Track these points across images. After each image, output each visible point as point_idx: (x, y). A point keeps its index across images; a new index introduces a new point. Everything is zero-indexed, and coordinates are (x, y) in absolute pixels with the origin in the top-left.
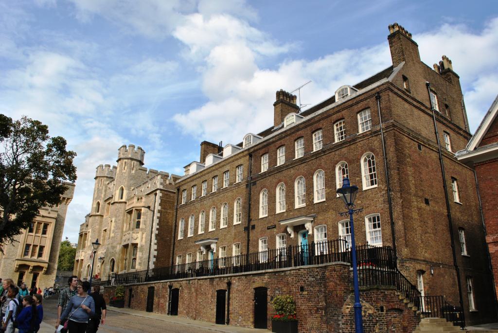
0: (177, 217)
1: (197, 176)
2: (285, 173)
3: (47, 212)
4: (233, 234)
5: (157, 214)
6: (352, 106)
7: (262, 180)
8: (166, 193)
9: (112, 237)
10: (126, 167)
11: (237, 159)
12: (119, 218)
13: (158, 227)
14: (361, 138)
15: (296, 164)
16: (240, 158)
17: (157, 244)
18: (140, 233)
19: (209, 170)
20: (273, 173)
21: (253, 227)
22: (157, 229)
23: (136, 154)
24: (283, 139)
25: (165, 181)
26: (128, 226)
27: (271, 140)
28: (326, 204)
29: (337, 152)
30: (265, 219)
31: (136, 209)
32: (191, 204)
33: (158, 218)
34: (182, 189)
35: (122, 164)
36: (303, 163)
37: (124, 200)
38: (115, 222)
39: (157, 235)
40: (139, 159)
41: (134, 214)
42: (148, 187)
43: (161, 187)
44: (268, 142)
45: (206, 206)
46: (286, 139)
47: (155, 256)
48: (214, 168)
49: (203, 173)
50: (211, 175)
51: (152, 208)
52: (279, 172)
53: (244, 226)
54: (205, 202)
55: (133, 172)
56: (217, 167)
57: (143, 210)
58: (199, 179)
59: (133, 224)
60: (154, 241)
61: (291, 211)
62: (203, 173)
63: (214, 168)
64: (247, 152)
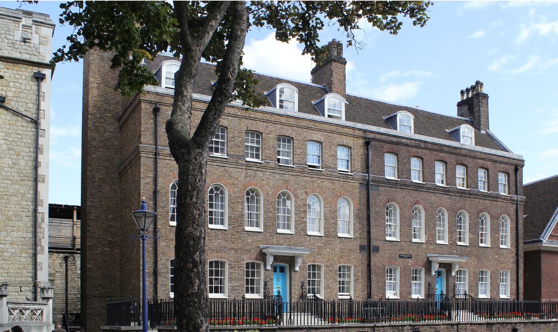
6: (496, 162)
7: (389, 189)
14: (502, 199)
20: (409, 188)
24: (420, 150)
27: (404, 141)
28: (469, 249)
29: (481, 201)
30: (395, 243)
44: (400, 140)
48: (283, 120)
52: (417, 190)
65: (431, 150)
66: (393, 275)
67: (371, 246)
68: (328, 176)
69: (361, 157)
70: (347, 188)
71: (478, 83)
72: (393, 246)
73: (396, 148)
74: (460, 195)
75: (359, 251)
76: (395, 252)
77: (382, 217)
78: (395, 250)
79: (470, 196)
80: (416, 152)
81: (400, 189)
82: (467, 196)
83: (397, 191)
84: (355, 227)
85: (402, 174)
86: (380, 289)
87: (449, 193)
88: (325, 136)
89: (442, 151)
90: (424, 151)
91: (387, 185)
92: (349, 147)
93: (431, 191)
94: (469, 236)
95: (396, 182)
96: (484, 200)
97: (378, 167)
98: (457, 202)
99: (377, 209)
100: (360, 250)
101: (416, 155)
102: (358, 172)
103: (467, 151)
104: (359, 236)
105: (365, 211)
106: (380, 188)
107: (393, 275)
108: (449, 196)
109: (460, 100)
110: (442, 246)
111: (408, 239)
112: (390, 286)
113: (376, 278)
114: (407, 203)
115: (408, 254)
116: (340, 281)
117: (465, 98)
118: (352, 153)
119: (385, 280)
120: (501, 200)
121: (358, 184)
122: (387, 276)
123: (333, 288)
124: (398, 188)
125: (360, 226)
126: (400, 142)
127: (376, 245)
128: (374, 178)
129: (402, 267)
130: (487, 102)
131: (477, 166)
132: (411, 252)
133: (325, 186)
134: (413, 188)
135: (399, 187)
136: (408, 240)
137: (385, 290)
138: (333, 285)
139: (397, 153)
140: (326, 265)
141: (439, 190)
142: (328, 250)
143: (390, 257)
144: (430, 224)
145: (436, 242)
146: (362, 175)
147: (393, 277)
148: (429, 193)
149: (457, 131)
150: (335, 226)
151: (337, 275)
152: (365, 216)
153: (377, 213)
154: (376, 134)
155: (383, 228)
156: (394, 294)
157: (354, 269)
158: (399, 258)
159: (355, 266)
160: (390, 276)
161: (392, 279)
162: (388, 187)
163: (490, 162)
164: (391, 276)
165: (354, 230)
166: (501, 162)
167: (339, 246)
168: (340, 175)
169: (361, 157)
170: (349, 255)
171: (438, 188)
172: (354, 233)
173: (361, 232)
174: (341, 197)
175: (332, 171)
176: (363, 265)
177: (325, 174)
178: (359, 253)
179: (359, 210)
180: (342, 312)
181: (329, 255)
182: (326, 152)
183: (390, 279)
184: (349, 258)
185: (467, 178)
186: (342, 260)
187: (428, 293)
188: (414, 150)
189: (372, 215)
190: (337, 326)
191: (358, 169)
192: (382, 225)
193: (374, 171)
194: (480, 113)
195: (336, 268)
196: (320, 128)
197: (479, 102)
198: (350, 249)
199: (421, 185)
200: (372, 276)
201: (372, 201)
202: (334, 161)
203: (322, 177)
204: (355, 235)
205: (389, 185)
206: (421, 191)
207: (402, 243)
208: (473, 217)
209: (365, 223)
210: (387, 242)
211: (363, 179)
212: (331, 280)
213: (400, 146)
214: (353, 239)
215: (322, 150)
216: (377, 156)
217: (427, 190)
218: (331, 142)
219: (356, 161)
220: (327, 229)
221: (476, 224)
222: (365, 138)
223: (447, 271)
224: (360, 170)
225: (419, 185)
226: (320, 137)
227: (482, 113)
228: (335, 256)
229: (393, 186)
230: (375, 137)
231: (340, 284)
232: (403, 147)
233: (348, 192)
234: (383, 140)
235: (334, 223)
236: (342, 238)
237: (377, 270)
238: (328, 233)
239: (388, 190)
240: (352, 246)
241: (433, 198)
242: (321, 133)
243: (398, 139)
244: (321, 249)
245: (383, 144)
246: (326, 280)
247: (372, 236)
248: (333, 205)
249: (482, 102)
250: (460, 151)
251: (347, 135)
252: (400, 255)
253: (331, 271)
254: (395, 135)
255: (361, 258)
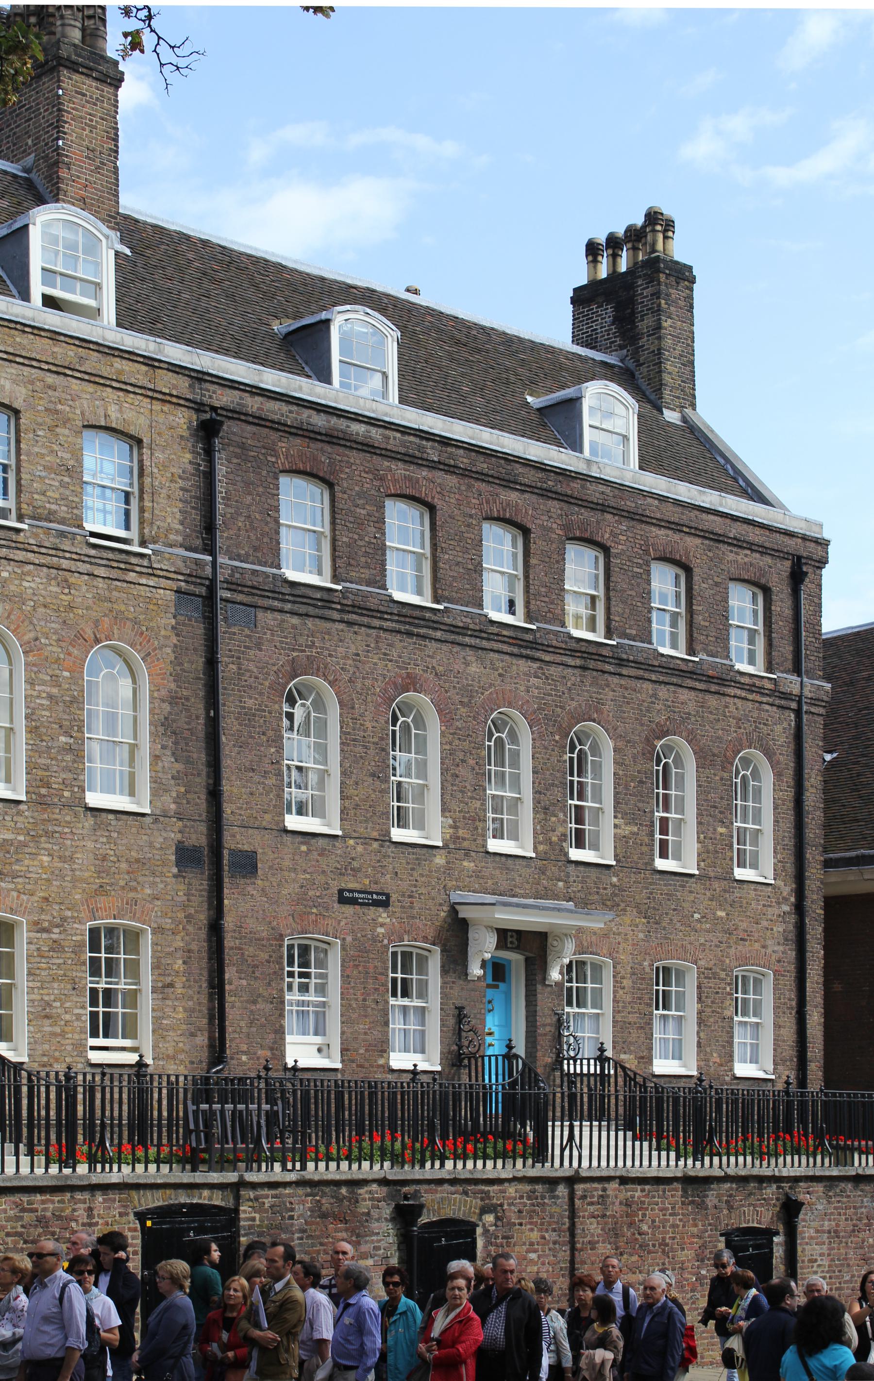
6: (718, 539)
7: (295, 620)
14: (742, 686)
20: (376, 623)
28: (615, 879)
29: (663, 692)
30: (321, 842)
44: (342, 424)
52: (410, 634)
53: (179, 836)
61: (467, 853)
65: (465, 473)
66: (313, 970)
67: (226, 852)
68: (43, 550)
69: (181, 483)
70: (123, 608)
71: (653, 217)
72: (315, 856)
73: (324, 455)
74: (578, 662)
75: (175, 870)
76: (320, 879)
77: (270, 733)
78: (324, 872)
79: (619, 670)
80: (410, 479)
81: (341, 626)
82: (608, 667)
83: (329, 634)
84: (159, 768)
85: (349, 564)
86: (263, 1026)
87: (538, 654)
88: (32, 383)
89: (509, 483)
90: (439, 476)
91: (288, 607)
92: (131, 437)
93: (467, 640)
94: (616, 826)
95: (326, 596)
96: (672, 688)
97: (254, 528)
98: (570, 689)
99: (250, 703)
100: (178, 863)
101: (408, 492)
102: (171, 546)
103: (608, 490)
104: (173, 806)
105: (198, 707)
106: (260, 614)
107: (313, 970)
108: (536, 665)
109: (583, 280)
110: (510, 861)
111: (373, 829)
112: (303, 1014)
113: (244, 982)
114: (368, 682)
115: (374, 888)
116: (94, 992)
117: (603, 272)
118: (147, 463)
119: (282, 990)
120: (739, 692)
121: (170, 596)
122: (291, 974)
123: (68, 1017)
124: (334, 621)
125: (179, 766)
126: (341, 435)
127: (246, 847)
128: (237, 575)
129: (349, 939)
130: (689, 299)
131: (647, 552)
132: (387, 883)
133: (30, 591)
134: (394, 625)
135: (336, 616)
136: (375, 834)
137: (280, 1032)
138: (68, 1005)
139: (331, 478)
140: (36, 923)
141: (497, 637)
142: (45, 859)
143: (301, 899)
144: (462, 771)
145: (485, 846)
146: (185, 559)
147: (314, 980)
148: (456, 649)
149: (572, 405)
150: (74, 761)
151: (84, 963)
152: (200, 726)
153: (247, 717)
154: (247, 395)
155: (271, 781)
156: (319, 1050)
157: (154, 944)
158: (336, 905)
159: (158, 930)
160: (302, 975)
161: (312, 988)
162: (293, 613)
163: (698, 541)
164: (307, 975)
165: (154, 780)
166: (739, 544)
167: (90, 845)
168: (93, 552)
169: (181, 483)
170: (134, 884)
171: (494, 630)
172: (155, 793)
173: (183, 789)
174: (97, 641)
175: (62, 534)
176: (190, 928)
177: (32, 541)
178: (175, 876)
179: (173, 699)
180: (103, 1125)
181: (48, 880)
182: (36, 449)
183: (304, 988)
184: (132, 895)
185: (608, 599)
186: (102, 901)
187: (455, 1048)
188: (399, 469)
189: (229, 724)
190: (85, 1183)
191: (169, 530)
192: (268, 767)
193: (238, 546)
194: (659, 338)
195: (79, 938)
196: (11, 350)
197: (657, 295)
198: (137, 861)
199: (428, 615)
200: (230, 973)
201: (227, 668)
202: (67, 492)
203: (20, 555)
204: (159, 804)
205: (296, 607)
206: (424, 637)
207: (351, 842)
208: (630, 751)
209: (200, 756)
210: (288, 839)
211: (189, 575)
212: (56, 985)
213: (341, 450)
214: (148, 820)
215: (18, 441)
216: (248, 484)
217: (452, 637)
218: (57, 412)
219: (162, 500)
220: (40, 773)
221: (641, 782)
222: (199, 407)
223: (527, 960)
224: (180, 539)
225: (417, 613)
226: (8, 385)
227: (668, 342)
228: (74, 887)
229: (311, 610)
230: (243, 406)
231: (94, 1003)
232: (355, 457)
233: (129, 623)
234: (272, 421)
235: (69, 749)
236: (104, 815)
237: (250, 950)
238: (43, 791)
239: (294, 627)
240: (146, 849)
241: (474, 668)
242: (13, 369)
243: (334, 420)
244: (17, 853)
245: (274, 435)
246: (39, 984)
247: (228, 809)
248: (66, 674)
249: (668, 295)
250: (583, 487)
251: (124, 387)
252: (341, 892)
253: (57, 947)
254: (323, 402)
255: (181, 897)
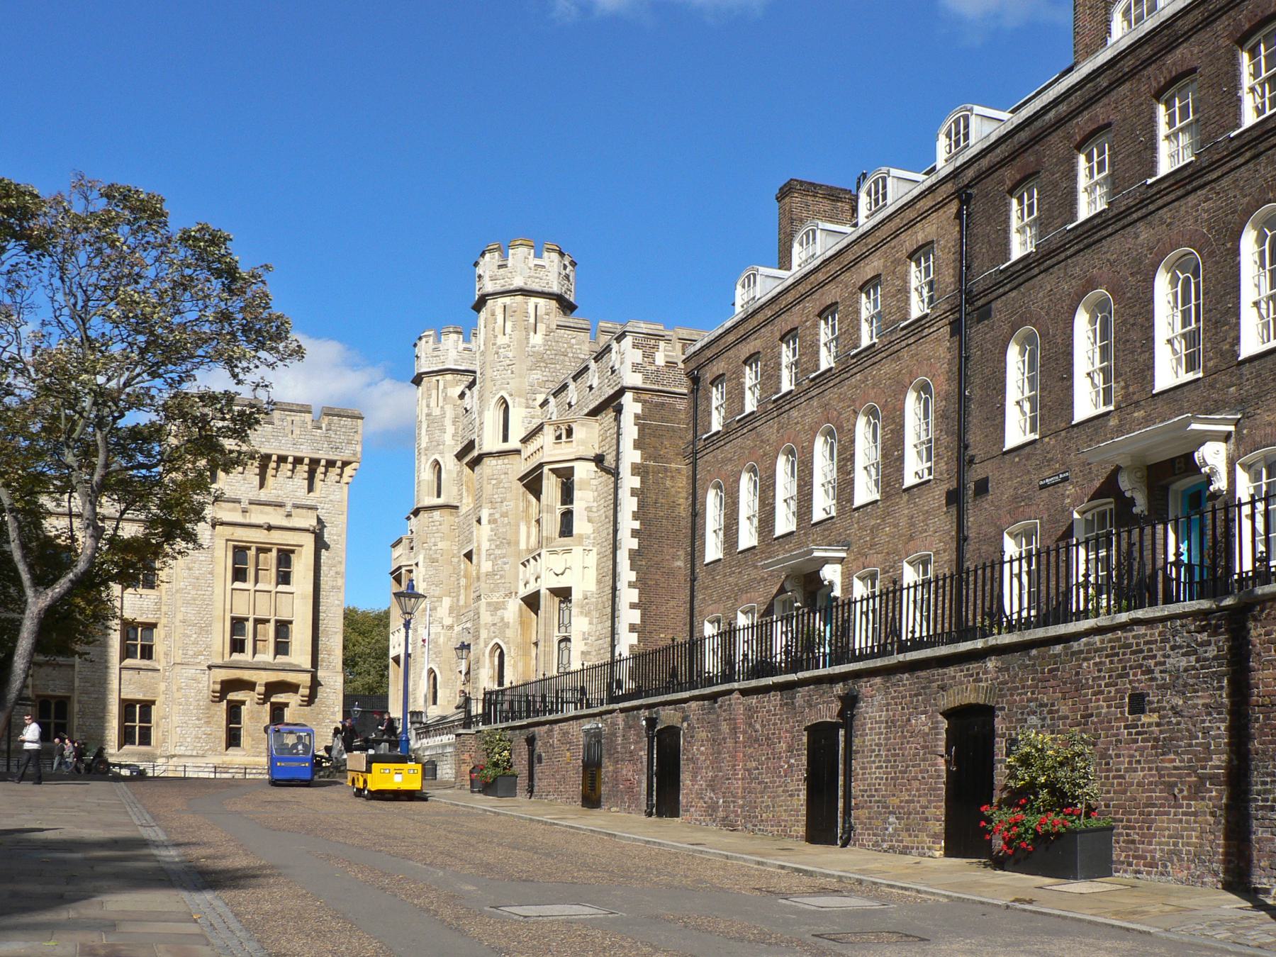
0: (699, 483)
1: (760, 317)
2: (1114, 247)
3: (281, 511)
4: (903, 522)
5: (630, 481)
8: (656, 399)
9: (487, 575)
10: (509, 324)
11: (911, 224)
12: (504, 509)
13: (637, 525)
15: (1160, 202)
16: (923, 216)
17: (641, 584)
18: (577, 550)
19: (801, 289)
20: (1063, 256)
21: (982, 488)
22: (635, 533)
23: (542, 273)
24: (1105, 100)
25: (649, 356)
26: (534, 530)
31: (552, 470)
32: (743, 427)
33: (634, 492)
34: (708, 375)
35: (493, 314)
36: (1195, 190)
37: (514, 443)
38: (489, 522)
39: (633, 555)
40: (555, 288)
41: (551, 486)
42: (591, 388)
43: (636, 380)
44: (1038, 124)
45: (799, 427)
46: (1114, 95)
47: (633, 628)
48: (821, 276)
49: (783, 302)
50: (812, 306)
51: (609, 461)
54: (794, 413)
55: (537, 339)
56: (834, 267)
57: (583, 472)
58: (769, 327)
59: (552, 523)
60: (627, 574)
62: (783, 302)
63: (821, 276)
64: (949, 188)
75: (945, 509)
87: (1205, 179)
93: (1135, 216)
111: (1061, 422)
129: (1045, 517)
134: (1076, 247)
168: (905, 332)
171: (1155, 190)
199: (1095, 222)
206: (1099, 241)
217: (1120, 224)
225: (1089, 225)
